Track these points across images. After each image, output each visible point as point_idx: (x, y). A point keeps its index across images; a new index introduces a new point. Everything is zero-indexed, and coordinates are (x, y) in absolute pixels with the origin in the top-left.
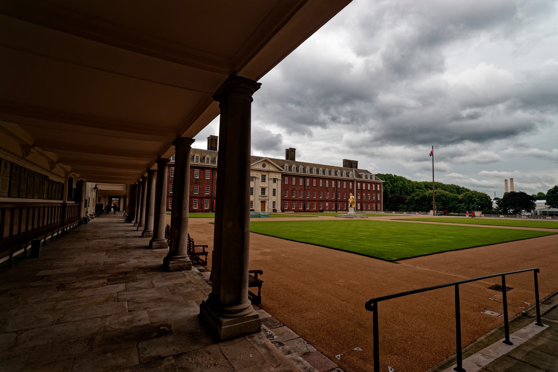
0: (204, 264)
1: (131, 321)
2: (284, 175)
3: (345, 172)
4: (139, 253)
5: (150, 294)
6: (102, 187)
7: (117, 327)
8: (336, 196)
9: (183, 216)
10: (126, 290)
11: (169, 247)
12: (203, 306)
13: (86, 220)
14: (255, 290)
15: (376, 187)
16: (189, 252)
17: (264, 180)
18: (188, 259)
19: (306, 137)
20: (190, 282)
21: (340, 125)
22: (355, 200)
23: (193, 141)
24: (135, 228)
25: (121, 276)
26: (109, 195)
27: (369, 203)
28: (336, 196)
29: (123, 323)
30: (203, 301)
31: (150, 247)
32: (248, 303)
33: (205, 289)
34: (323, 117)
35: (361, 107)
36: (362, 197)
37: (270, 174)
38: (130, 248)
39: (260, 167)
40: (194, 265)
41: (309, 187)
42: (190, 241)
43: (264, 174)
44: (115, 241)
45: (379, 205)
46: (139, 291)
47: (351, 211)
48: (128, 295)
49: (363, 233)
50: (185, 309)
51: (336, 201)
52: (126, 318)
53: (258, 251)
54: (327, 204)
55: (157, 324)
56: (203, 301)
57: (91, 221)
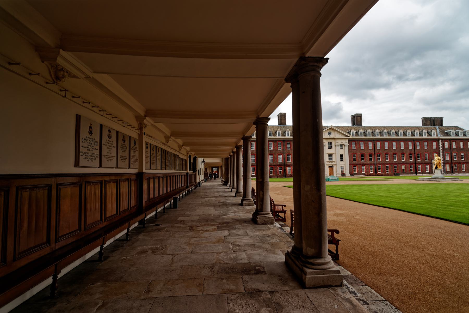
0: (284, 220)
1: (235, 259)
2: (350, 141)
4: (235, 208)
5: (245, 240)
6: (208, 160)
7: (227, 262)
8: (415, 158)
9: (265, 181)
10: (230, 235)
11: (255, 206)
12: (288, 255)
13: (199, 184)
14: (333, 248)
16: (271, 211)
18: (271, 215)
19: (368, 102)
20: (274, 234)
21: (408, 83)
22: (441, 162)
23: (269, 119)
24: (230, 190)
25: (225, 225)
26: (212, 166)
27: (463, 164)
29: (231, 259)
30: (287, 251)
31: (241, 204)
32: (329, 258)
33: (287, 242)
34: (385, 78)
35: (434, 58)
36: (451, 157)
37: (337, 141)
38: (229, 205)
40: (276, 220)
41: (380, 152)
42: (271, 200)
43: (330, 141)
44: (219, 199)
46: (238, 237)
47: (437, 174)
48: (231, 239)
49: (458, 199)
50: (273, 255)
52: (232, 256)
53: (335, 212)
54: (403, 167)
55: (254, 264)
56: (287, 251)
57: (203, 184)
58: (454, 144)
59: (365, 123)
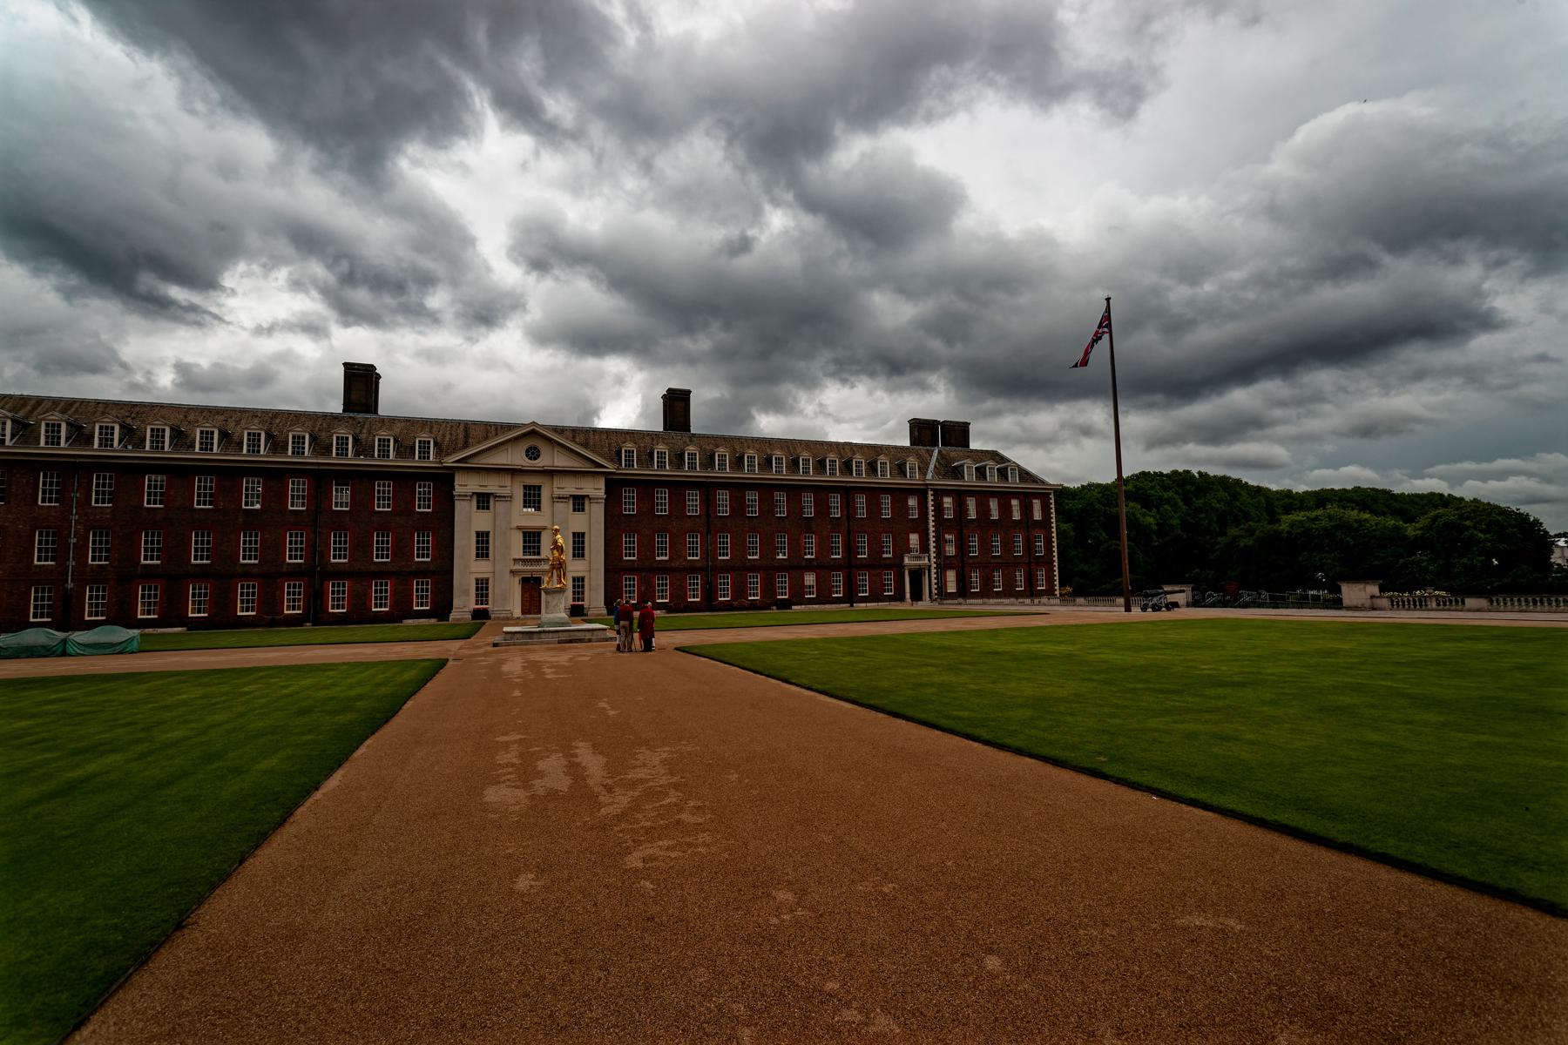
2: (614, 486)
3: (911, 461)
8: (850, 549)
15: (1026, 509)
27: (998, 567)
28: (850, 549)
36: (962, 547)
37: (557, 482)
39: (516, 457)
45: (1041, 574)
51: (850, 566)
54: (810, 579)
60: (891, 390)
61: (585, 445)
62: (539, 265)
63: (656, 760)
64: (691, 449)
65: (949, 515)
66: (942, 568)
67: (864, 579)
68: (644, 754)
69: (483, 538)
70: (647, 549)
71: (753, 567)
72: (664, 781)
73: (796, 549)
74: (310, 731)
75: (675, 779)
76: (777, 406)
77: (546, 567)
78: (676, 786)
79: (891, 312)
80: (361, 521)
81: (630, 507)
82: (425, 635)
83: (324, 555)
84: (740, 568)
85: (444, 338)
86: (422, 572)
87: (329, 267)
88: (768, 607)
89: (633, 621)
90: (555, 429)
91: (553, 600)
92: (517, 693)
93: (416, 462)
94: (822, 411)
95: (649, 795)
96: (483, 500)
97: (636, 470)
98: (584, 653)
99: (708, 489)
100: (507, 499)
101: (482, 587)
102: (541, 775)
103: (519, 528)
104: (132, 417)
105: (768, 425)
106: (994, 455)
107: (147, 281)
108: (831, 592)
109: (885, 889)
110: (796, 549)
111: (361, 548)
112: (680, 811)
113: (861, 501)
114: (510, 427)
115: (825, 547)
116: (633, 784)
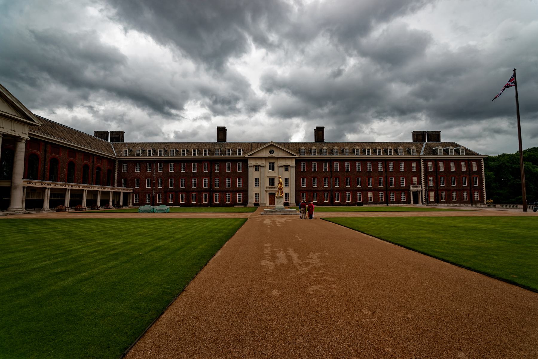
2: (298, 162)
8: (387, 183)
15: (469, 166)
17: (272, 167)
27: (454, 191)
28: (387, 183)
36: (437, 182)
37: (280, 161)
39: (266, 153)
43: (272, 161)
45: (477, 194)
51: (387, 190)
58: (452, 165)
59: (328, 138)
60: (400, 121)
61: (288, 148)
62: (269, 90)
63: (316, 257)
64: (325, 148)
65: (431, 169)
66: (428, 191)
67: (393, 195)
68: (311, 254)
69: (257, 180)
70: (310, 183)
71: (348, 190)
72: (319, 264)
73: (365, 183)
74: (211, 238)
75: (323, 264)
76: (354, 130)
77: (277, 189)
78: (324, 267)
79: (399, 91)
80: (222, 176)
81: (304, 169)
82: (241, 211)
83: (213, 185)
84: (343, 190)
85: (242, 117)
86: (239, 191)
87: (210, 99)
88: (354, 205)
89: (306, 208)
90: (279, 143)
91: (279, 200)
92: (269, 231)
93: (237, 156)
94: (372, 131)
95: (314, 269)
96: (257, 168)
97: (305, 156)
98: (289, 219)
99: (331, 162)
100: (264, 167)
101: (257, 196)
102: (278, 258)
103: (268, 177)
104: (166, 146)
105: (351, 138)
106: (453, 144)
107: (167, 108)
108: (379, 200)
109: (409, 316)
110: (365, 183)
111: (223, 183)
112: (326, 275)
113: (391, 165)
114: (264, 144)
115: (376, 183)
116: (308, 264)
